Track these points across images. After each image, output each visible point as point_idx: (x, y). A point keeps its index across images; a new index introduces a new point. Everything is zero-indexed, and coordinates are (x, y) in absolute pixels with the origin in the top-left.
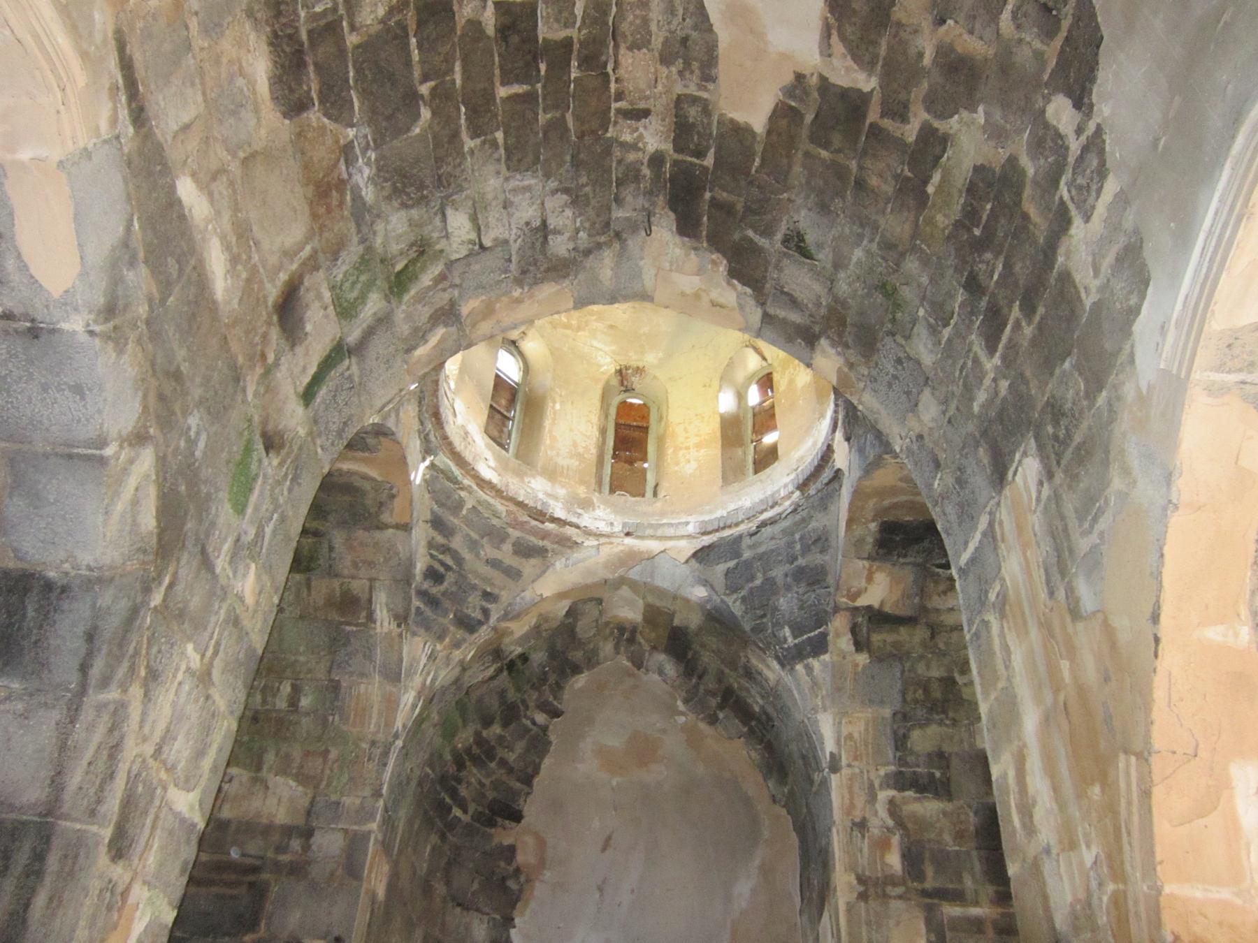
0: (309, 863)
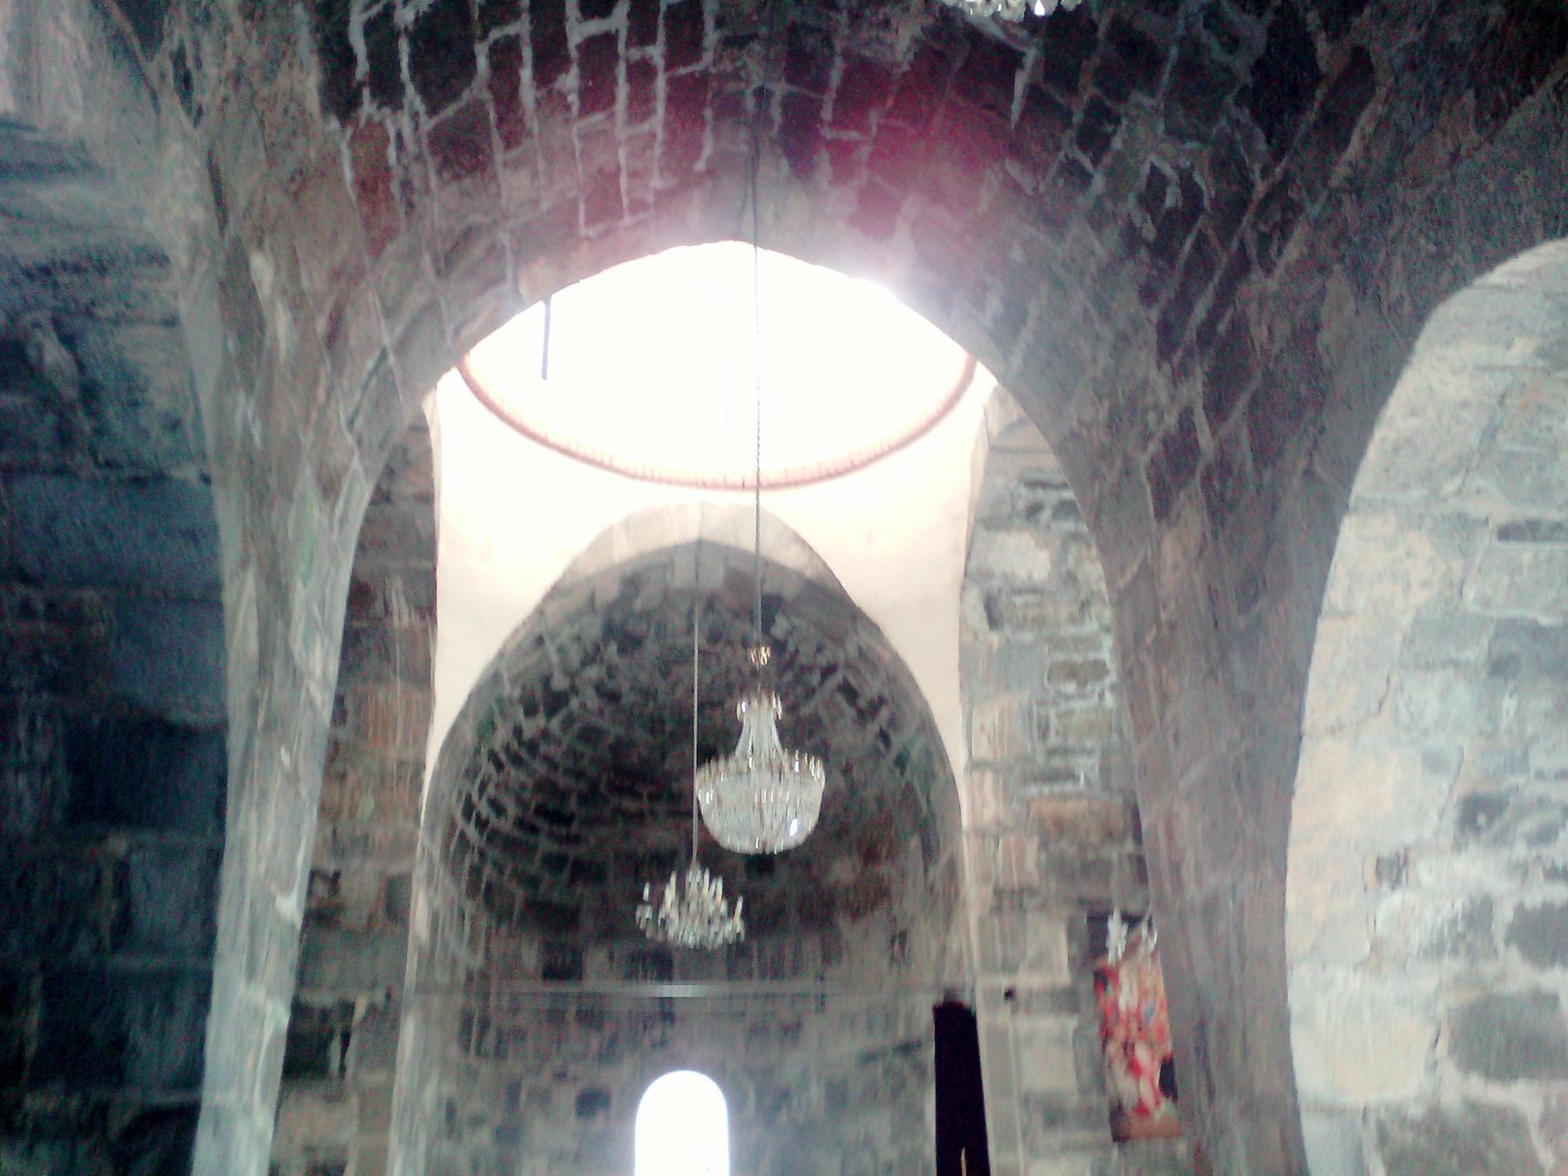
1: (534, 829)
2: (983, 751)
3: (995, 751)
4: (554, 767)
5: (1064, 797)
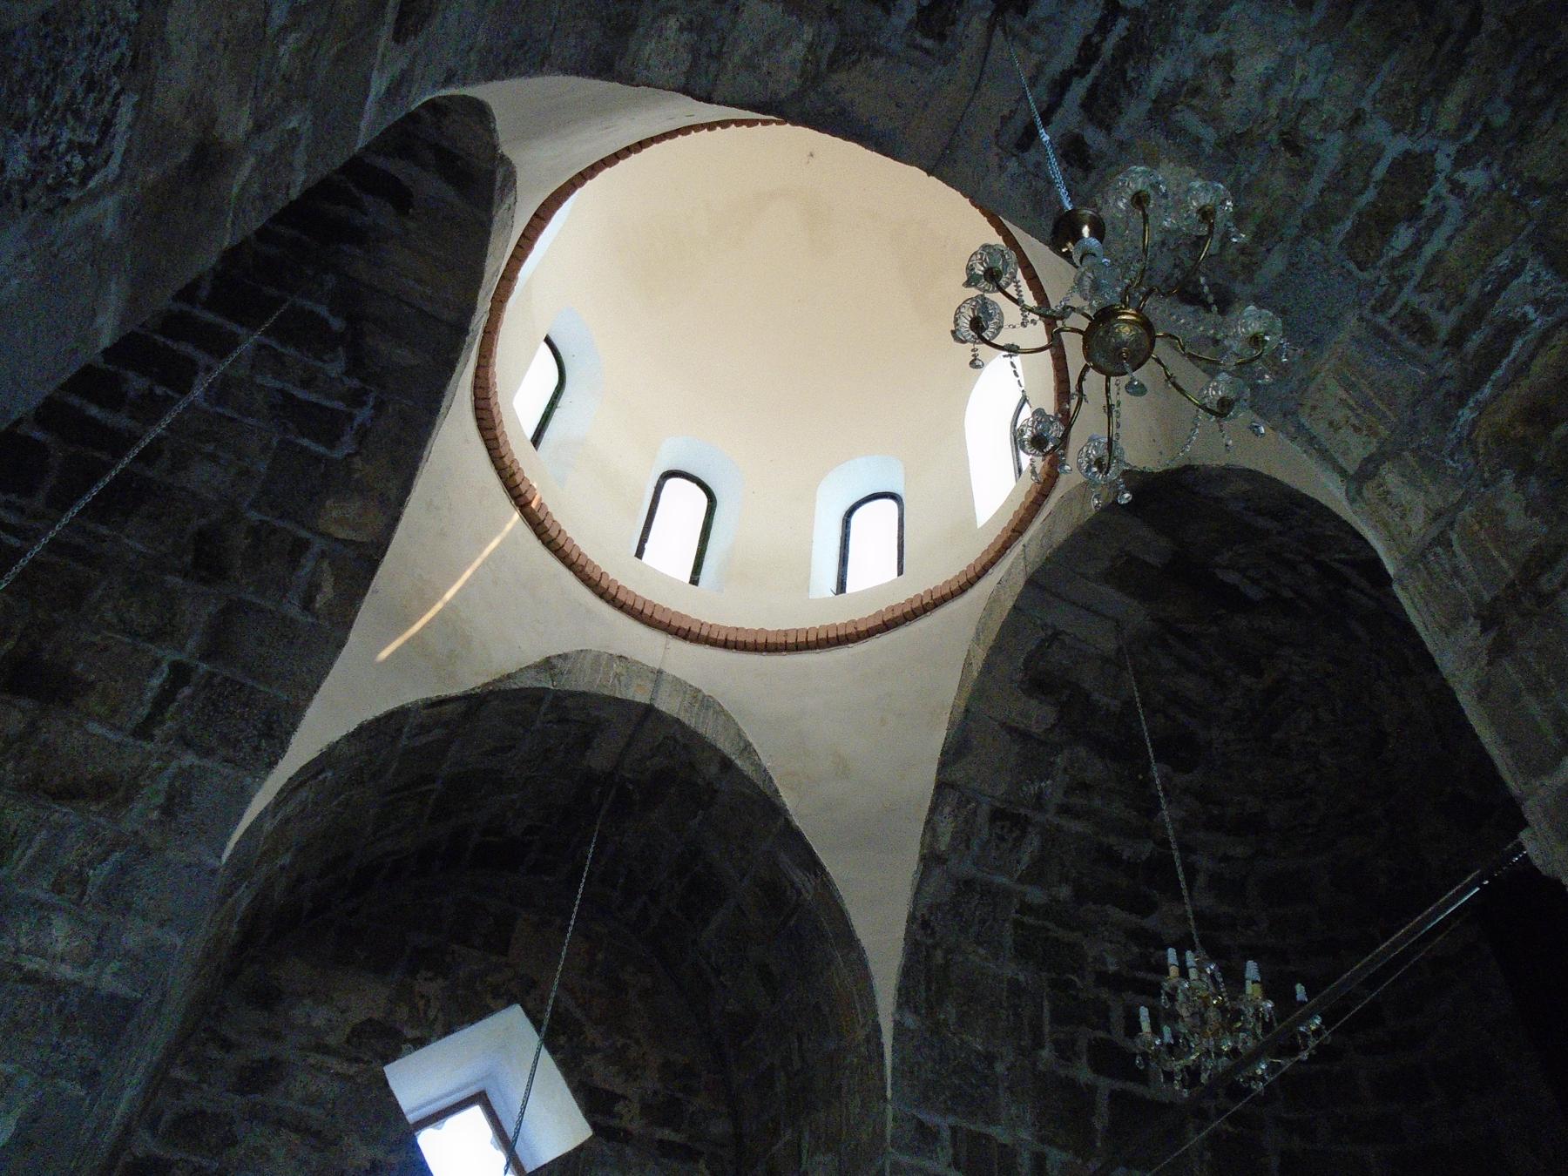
2: (1356, 449)
3: (1372, 432)
5: (1522, 369)
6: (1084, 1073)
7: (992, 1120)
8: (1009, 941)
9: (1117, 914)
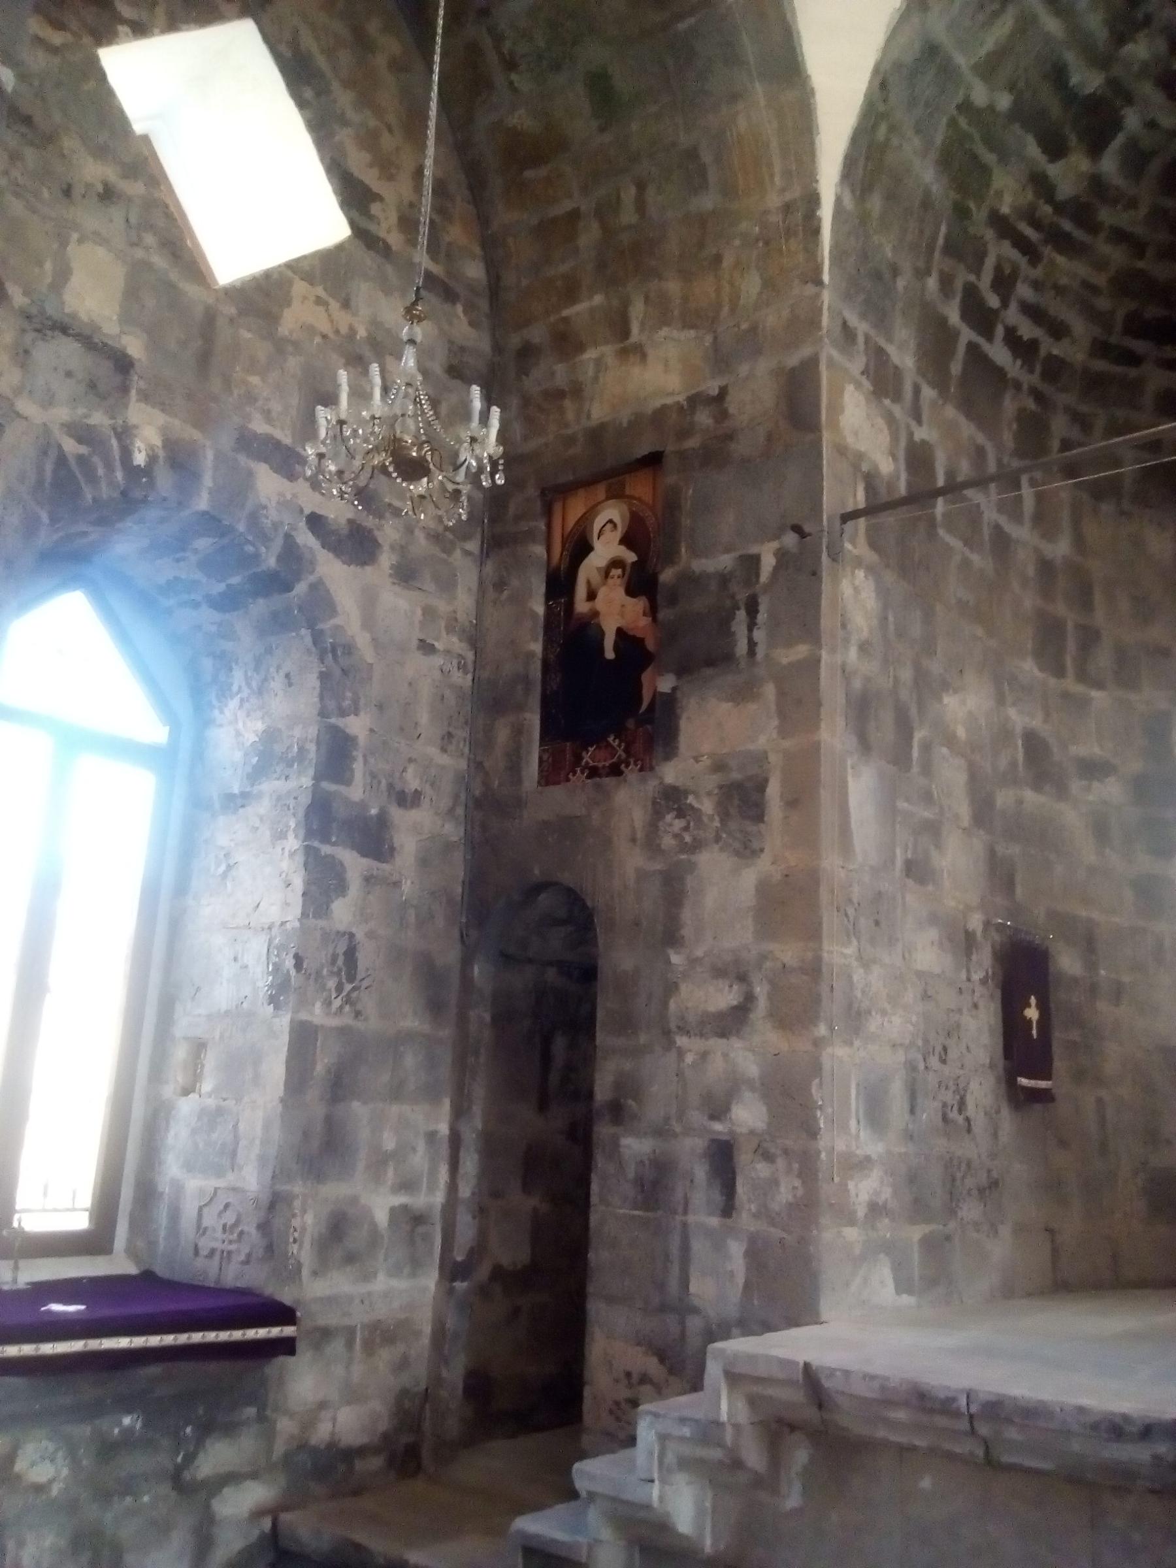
0: (730, 437)
1: (1134, 360)
4: (1138, 248)
6: (954, 316)
7: (890, 340)
8: (939, 139)
9: (1033, 149)
